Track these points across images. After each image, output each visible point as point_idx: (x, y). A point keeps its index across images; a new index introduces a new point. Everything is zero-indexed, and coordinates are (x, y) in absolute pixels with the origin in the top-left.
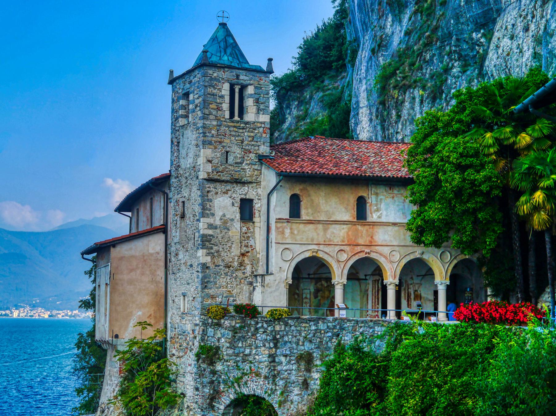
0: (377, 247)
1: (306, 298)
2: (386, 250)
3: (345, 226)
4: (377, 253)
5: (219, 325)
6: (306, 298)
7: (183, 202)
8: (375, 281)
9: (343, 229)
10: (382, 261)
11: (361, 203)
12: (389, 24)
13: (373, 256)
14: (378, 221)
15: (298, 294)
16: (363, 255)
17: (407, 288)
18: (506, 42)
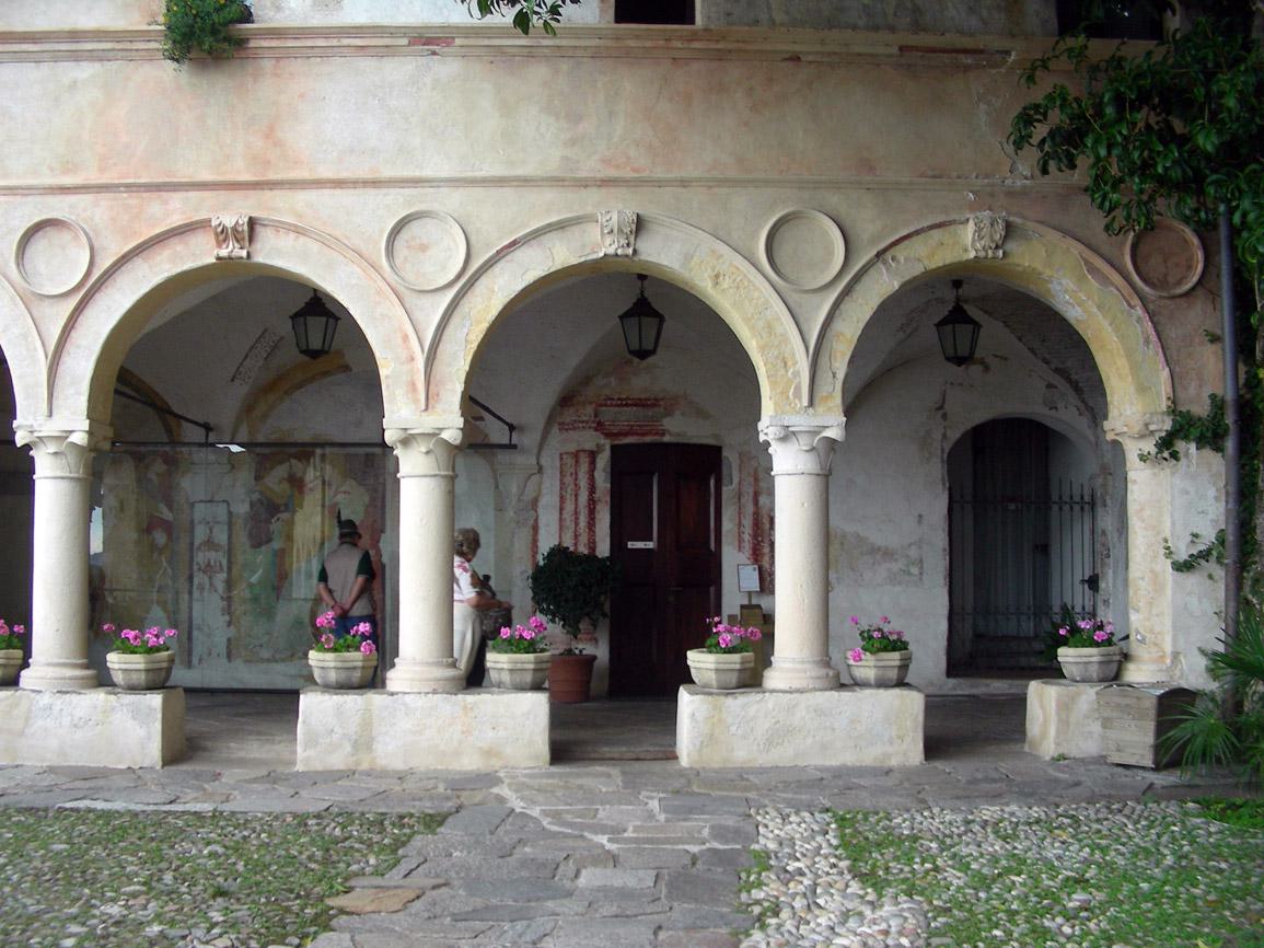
0: (302, 198)
1: (210, 544)
3: (86, 71)
4: (299, 231)
6: (210, 544)
8: (576, 455)
9: (74, 85)
14: (318, 20)
15: (168, 527)
16: (202, 253)
17: (749, 490)
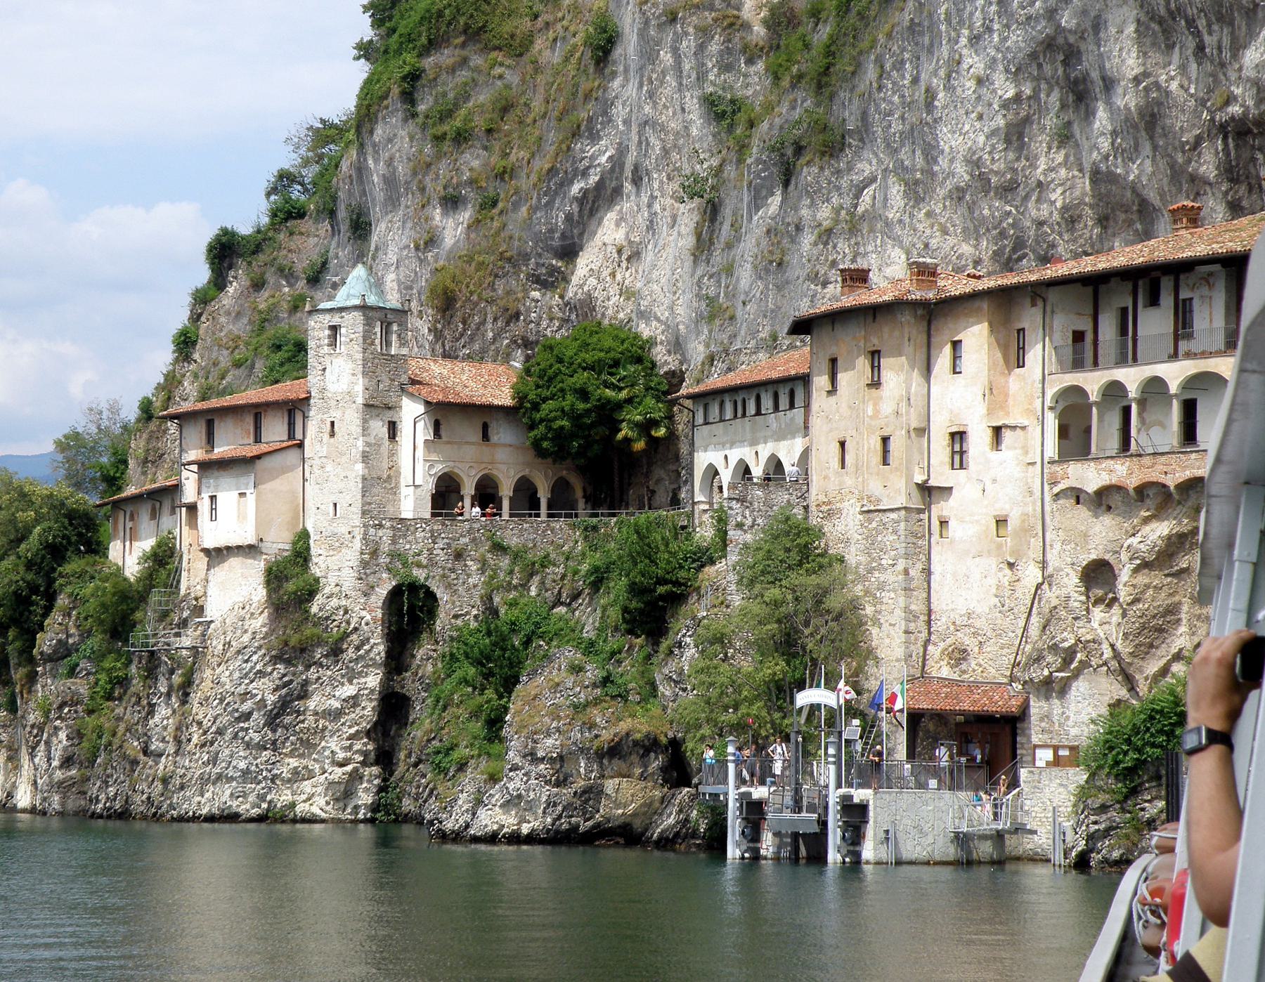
2: (504, 468)
5: (381, 526)
7: (333, 423)
10: (500, 476)
11: (485, 428)
12: (438, 218)
13: (495, 472)
18: (592, 281)
